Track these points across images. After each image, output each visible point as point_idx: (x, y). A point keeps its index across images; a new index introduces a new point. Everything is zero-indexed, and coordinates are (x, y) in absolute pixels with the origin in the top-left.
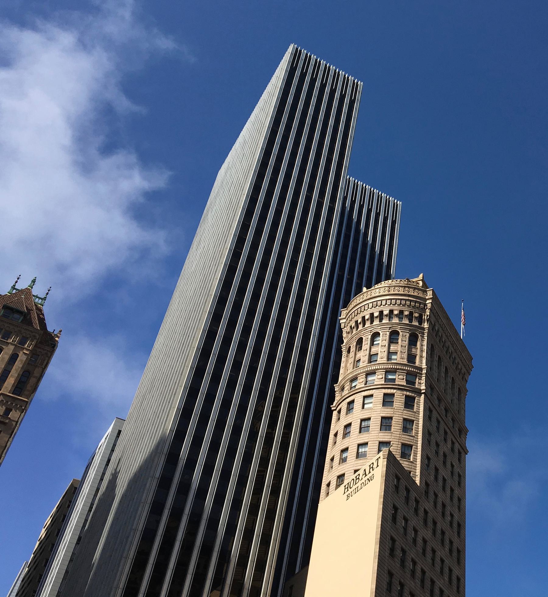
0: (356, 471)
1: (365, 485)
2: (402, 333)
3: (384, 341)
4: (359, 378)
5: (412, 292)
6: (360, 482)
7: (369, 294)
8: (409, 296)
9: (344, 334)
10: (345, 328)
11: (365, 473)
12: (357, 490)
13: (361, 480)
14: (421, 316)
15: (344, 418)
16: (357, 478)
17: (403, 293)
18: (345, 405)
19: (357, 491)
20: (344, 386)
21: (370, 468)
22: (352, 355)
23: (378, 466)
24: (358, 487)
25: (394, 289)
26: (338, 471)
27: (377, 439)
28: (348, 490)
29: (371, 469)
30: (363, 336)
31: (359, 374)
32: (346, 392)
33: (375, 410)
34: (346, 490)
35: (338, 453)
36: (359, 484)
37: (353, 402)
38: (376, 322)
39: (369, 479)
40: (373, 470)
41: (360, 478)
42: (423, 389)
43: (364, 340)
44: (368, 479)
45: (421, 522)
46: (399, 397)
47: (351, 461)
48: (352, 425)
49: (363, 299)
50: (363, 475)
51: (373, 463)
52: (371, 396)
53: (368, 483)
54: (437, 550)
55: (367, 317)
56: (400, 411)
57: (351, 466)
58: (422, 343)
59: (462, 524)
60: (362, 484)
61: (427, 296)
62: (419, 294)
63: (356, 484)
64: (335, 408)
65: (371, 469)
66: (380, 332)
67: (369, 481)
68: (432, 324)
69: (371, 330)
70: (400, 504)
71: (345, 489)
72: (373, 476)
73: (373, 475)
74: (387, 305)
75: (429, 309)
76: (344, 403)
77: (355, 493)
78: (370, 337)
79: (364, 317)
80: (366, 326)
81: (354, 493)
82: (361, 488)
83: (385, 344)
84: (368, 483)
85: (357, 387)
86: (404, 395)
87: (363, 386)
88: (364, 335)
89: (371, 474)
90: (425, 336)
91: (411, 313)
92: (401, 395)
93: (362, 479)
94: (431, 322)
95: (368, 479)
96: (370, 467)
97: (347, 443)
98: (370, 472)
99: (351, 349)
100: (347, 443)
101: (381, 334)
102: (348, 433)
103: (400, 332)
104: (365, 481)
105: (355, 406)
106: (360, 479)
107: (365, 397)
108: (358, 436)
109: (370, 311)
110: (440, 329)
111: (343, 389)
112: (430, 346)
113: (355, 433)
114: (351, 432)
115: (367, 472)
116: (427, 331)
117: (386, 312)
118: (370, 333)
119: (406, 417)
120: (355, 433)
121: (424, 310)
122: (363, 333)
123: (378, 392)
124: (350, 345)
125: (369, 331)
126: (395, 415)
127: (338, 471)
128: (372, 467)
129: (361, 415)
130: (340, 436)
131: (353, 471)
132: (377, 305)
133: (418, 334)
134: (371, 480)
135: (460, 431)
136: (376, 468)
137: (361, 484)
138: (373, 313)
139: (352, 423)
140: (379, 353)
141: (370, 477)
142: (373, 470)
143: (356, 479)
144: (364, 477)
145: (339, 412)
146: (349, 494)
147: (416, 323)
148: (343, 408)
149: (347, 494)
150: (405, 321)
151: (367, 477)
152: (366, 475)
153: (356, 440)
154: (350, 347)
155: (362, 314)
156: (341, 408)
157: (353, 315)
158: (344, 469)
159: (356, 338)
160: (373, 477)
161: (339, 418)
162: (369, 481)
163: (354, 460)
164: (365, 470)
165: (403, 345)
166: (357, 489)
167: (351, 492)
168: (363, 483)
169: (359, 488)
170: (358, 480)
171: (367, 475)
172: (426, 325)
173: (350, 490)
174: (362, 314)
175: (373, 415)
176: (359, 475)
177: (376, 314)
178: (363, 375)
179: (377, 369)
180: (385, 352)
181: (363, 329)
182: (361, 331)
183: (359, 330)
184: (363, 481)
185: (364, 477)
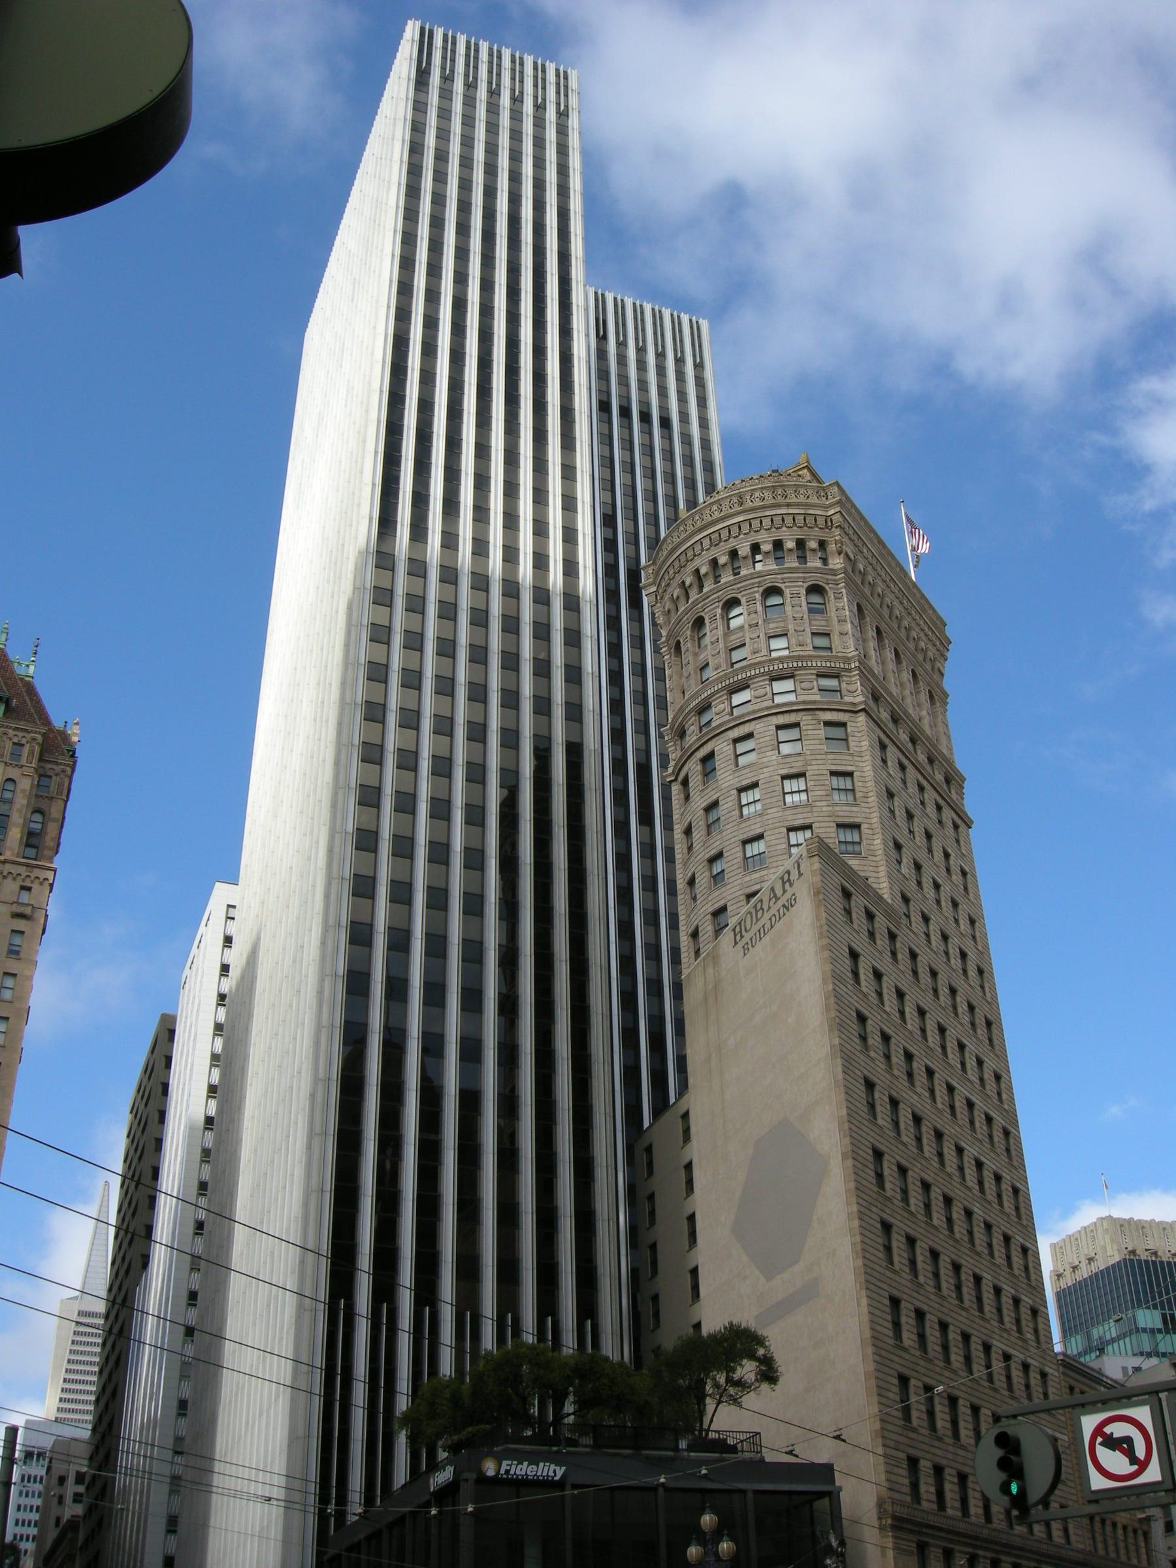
0: (749, 896)
1: (780, 918)
2: (788, 590)
3: (754, 615)
4: (713, 704)
5: (793, 495)
6: (767, 916)
7: (698, 518)
8: (788, 505)
9: (659, 617)
10: (659, 605)
11: (775, 896)
12: (762, 932)
13: (768, 910)
14: (822, 544)
15: (698, 793)
16: (758, 908)
17: (773, 501)
18: (694, 765)
19: (765, 934)
20: (684, 726)
21: (784, 883)
22: (685, 659)
23: (800, 874)
24: (763, 926)
25: (751, 496)
26: (710, 904)
27: (782, 824)
28: (742, 937)
29: (787, 885)
30: (703, 614)
31: (712, 695)
32: (691, 738)
34: (738, 937)
35: (701, 866)
36: (765, 920)
37: (711, 756)
38: (727, 577)
39: (786, 904)
40: (791, 885)
41: (765, 907)
42: (860, 703)
43: (707, 621)
44: (784, 906)
45: (908, 976)
46: (810, 727)
47: (737, 877)
48: (721, 803)
49: (687, 533)
51: (788, 872)
52: (750, 736)
53: (784, 914)
54: (948, 1027)
55: (703, 571)
56: (818, 757)
58: (837, 605)
59: (985, 969)
60: (773, 919)
61: (827, 499)
62: (808, 497)
63: (757, 920)
64: (673, 778)
65: (787, 885)
66: (739, 596)
67: (788, 909)
68: (850, 559)
69: (718, 597)
70: (861, 944)
72: (793, 897)
73: (794, 895)
74: (742, 536)
75: (837, 527)
76: (692, 763)
77: (761, 939)
78: (719, 611)
79: (697, 571)
80: (705, 590)
81: (758, 939)
82: (772, 927)
83: (756, 622)
84: (784, 914)
85: (714, 724)
86: (822, 723)
87: (727, 718)
88: (706, 610)
89: (788, 895)
90: (841, 588)
91: (801, 544)
92: (815, 722)
93: (769, 908)
94: (847, 555)
95: (784, 906)
96: (783, 880)
97: (718, 843)
98: (785, 891)
99: (682, 643)
100: (718, 843)
101: (743, 601)
102: (714, 822)
103: (784, 589)
104: (778, 911)
105: (717, 764)
106: (766, 909)
107: (736, 741)
108: (739, 823)
109: (707, 556)
110: (869, 569)
111: (682, 734)
112: (856, 608)
113: (731, 820)
114: (722, 819)
115: (779, 892)
116: (843, 575)
117: (744, 550)
118: (717, 604)
119: (834, 768)
120: (731, 820)
121: (827, 530)
122: (702, 607)
123: (762, 725)
124: (678, 638)
125: (715, 599)
126: (809, 768)
127: (710, 904)
128: (789, 880)
129: (736, 780)
130: (698, 835)
131: (743, 898)
132: (720, 540)
133: (824, 585)
134: (792, 906)
135: (948, 781)
136: (798, 879)
137: (770, 919)
138: (715, 558)
139: (720, 799)
140: (747, 640)
141: (787, 901)
142: (791, 885)
143: (757, 912)
145: (685, 783)
146: (747, 943)
147: (814, 563)
148: (692, 773)
149: (741, 944)
150: (792, 562)
151: (780, 903)
152: (777, 899)
153: (736, 833)
154: (678, 643)
155: (691, 567)
156: (687, 776)
157: (671, 572)
158: (721, 897)
159: (687, 619)
160: (795, 899)
161: (689, 795)
162: (788, 909)
163: (740, 876)
164: (772, 889)
165: (797, 615)
166: (762, 929)
167: (751, 939)
168: (774, 915)
169: (768, 926)
170: (760, 914)
171: (779, 898)
172: (836, 562)
173: (747, 936)
174: (691, 567)
175: (761, 776)
176: (761, 901)
177: (723, 560)
178: (721, 696)
180: (759, 637)
181: (701, 597)
182: (696, 603)
183: (690, 601)
184: (774, 911)
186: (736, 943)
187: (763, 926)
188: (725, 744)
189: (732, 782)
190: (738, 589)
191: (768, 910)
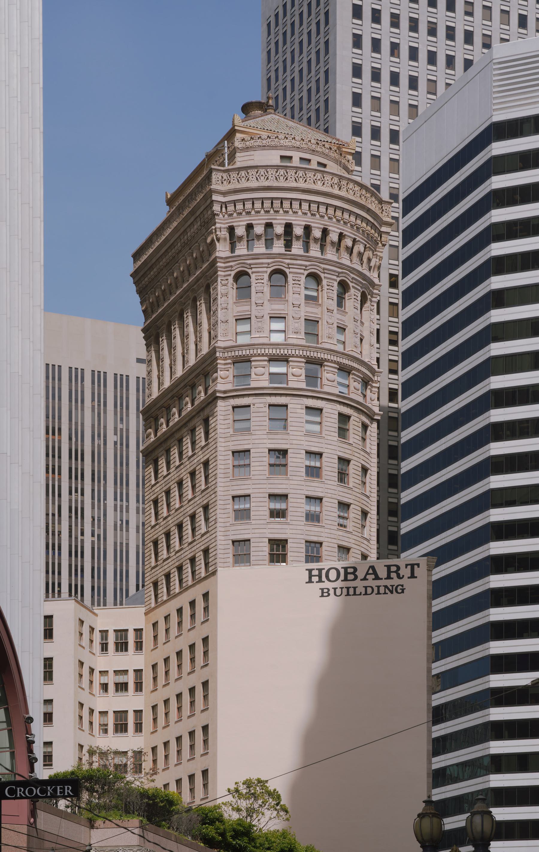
18: (262, 405)
19: (355, 594)
23: (413, 576)
29: (393, 575)
33: (330, 442)
44: (386, 587)
50: (367, 573)
57: (299, 532)
71: (310, 576)
73: (402, 586)
93: (365, 579)
128: (397, 572)
129: (307, 443)
141: (392, 586)
144: (373, 579)
175: (326, 450)
179: (328, 361)
185: (373, 579)
186: (310, 581)
187: (355, 588)
188: (299, 406)
189: (302, 443)
190: (324, 269)
191: (361, 580)
